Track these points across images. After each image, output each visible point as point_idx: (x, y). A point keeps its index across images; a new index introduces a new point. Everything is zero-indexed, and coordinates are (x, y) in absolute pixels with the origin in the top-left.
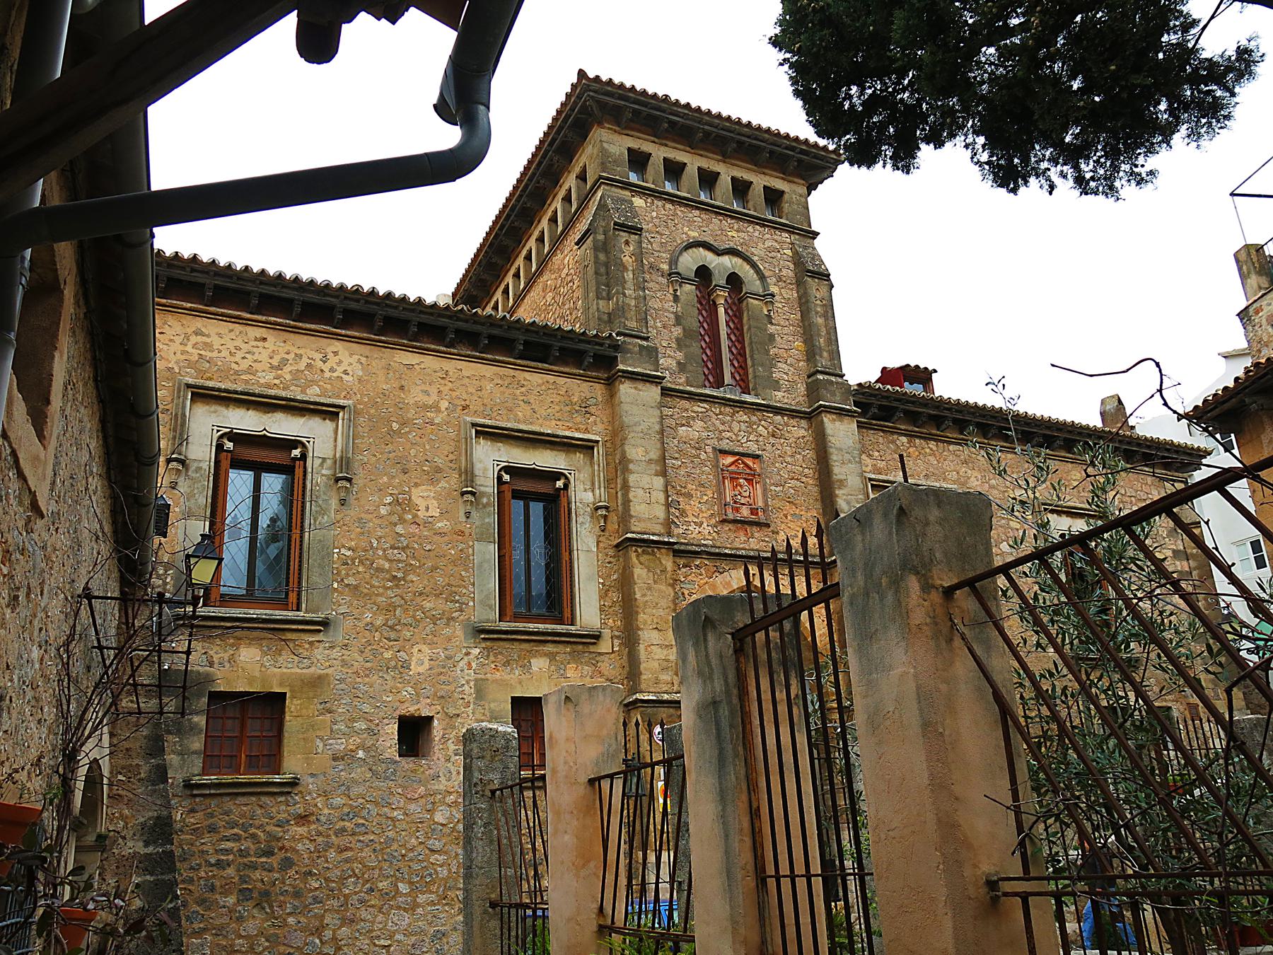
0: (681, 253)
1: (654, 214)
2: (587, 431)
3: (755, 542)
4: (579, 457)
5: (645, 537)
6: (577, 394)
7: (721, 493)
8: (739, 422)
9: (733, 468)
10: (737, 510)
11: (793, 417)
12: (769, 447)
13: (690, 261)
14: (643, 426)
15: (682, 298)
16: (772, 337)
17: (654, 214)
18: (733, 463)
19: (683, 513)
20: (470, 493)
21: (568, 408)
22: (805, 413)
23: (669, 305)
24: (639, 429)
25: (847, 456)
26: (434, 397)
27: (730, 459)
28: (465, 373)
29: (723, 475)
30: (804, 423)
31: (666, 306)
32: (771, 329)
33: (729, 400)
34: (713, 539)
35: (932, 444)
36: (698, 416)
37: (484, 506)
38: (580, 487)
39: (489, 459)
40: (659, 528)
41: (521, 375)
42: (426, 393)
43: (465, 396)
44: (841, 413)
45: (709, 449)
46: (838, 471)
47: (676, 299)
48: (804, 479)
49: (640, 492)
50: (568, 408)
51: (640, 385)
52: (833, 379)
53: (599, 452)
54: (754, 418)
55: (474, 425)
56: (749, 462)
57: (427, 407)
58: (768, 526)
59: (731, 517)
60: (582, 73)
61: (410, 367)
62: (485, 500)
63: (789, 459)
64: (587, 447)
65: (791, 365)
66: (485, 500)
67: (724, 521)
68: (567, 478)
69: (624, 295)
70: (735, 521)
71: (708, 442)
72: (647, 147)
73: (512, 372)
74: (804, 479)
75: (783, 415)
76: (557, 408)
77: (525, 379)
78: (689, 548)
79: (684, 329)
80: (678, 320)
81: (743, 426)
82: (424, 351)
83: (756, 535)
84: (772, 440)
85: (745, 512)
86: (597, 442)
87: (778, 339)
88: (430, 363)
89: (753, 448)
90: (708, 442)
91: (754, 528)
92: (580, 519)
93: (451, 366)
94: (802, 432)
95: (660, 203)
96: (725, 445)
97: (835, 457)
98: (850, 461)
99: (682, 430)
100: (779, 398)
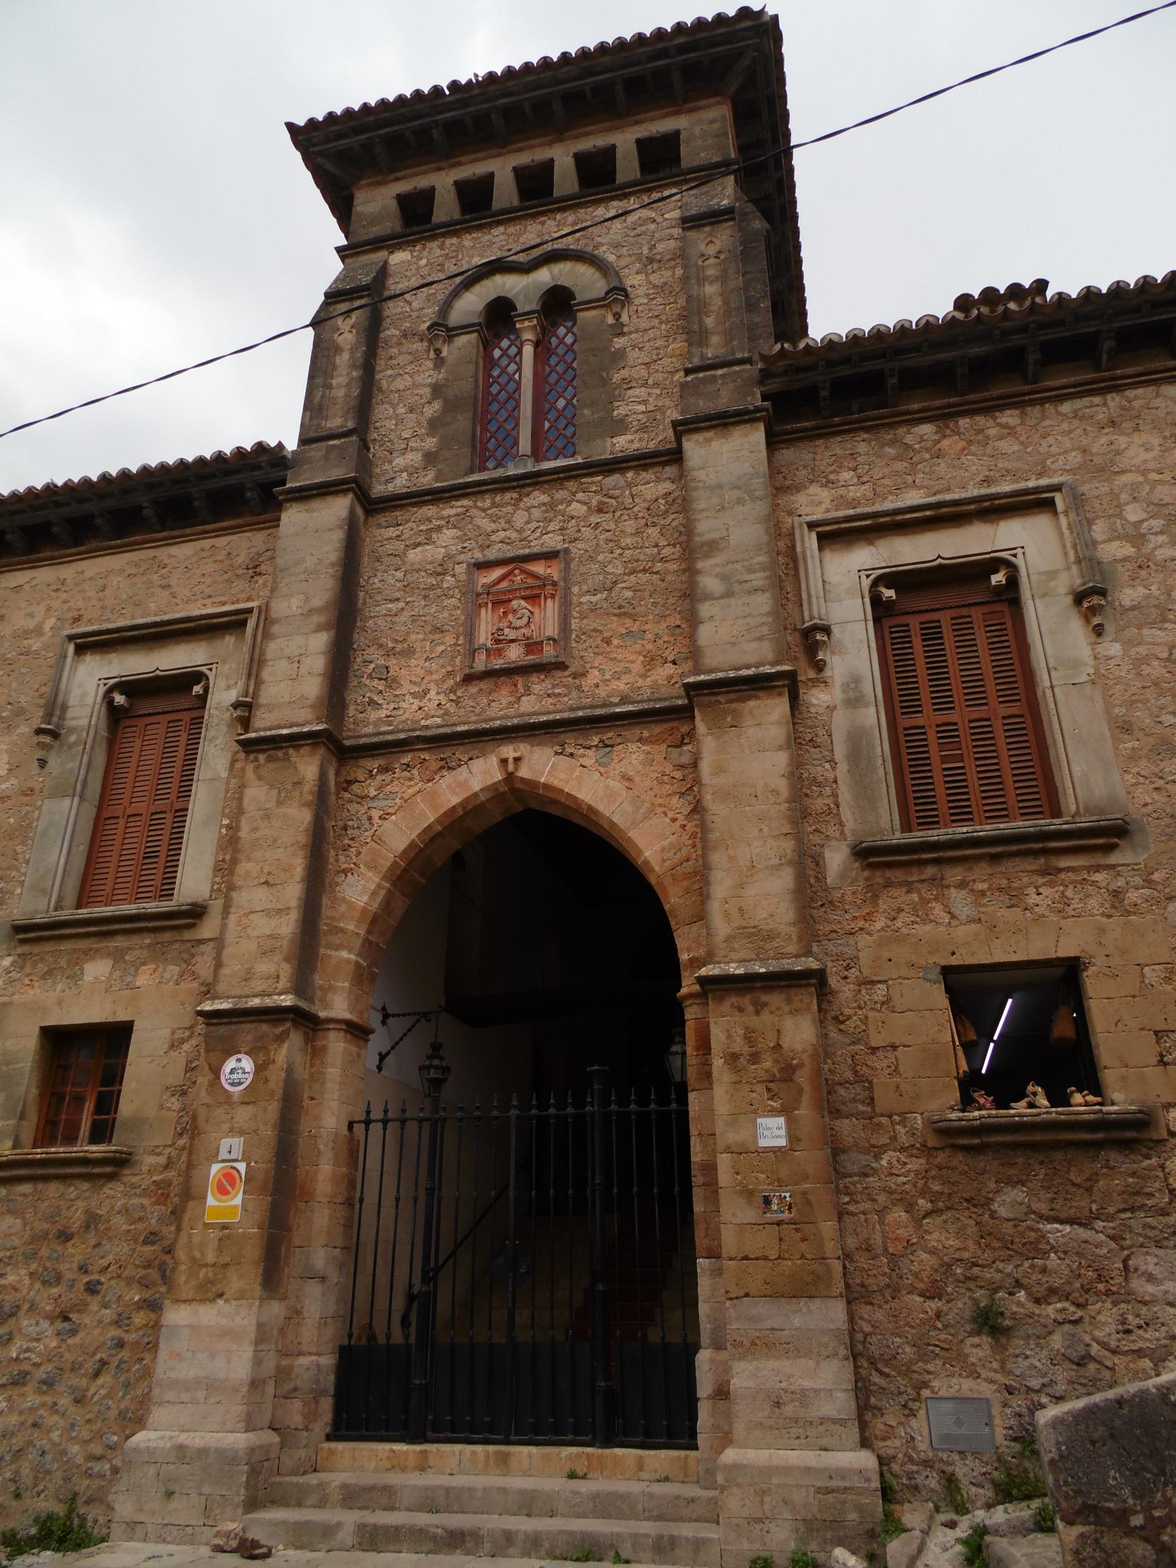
0: (455, 294)
1: (424, 261)
2: (249, 599)
3: (536, 701)
4: (229, 641)
5: (273, 732)
6: (243, 554)
7: (470, 632)
8: (528, 510)
9: (504, 585)
10: (499, 653)
11: (645, 468)
12: (587, 532)
13: (472, 303)
14: (310, 562)
15: (450, 360)
16: (621, 354)
17: (424, 261)
18: (503, 578)
19: (391, 682)
20: (51, 733)
21: (225, 577)
22: (668, 452)
23: (428, 375)
24: (301, 568)
25: (737, 493)
26: (39, 618)
27: (498, 572)
28: (88, 575)
29: (476, 600)
30: (670, 471)
31: (419, 379)
32: (619, 343)
33: (509, 479)
34: (447, 713)
35: (1010, 417)
36: (448, 523)
37: (70, 747)
38: (222, 683)
39: (89, 681)
40: (304, 714)
41: (163, 553)
42: (31, 615)
43: (80, 604)
44: (723, 421)
45: (460, 569)
46: (706, 527)
47: (439, 361)
48: (659, 566)
49: (284, 663)
50: (225, 577)
51: (316, 504)
52: (720, 372)
53: (251, 624)
54: (561, 494)
55: (71, 638)
56: (539, 568)
57: (26, 634)
58: (561, 666)
59: (481, 663)
60: (290, 126)
61: (18, 588)
62: (73, 738)
63: (629, 541)
64: (234, 623)
65: (656, 385)
66: (73, 738)
67: (469, 679)
68: (208, 679)
69: (330, 387)
70: (490, 674)
71: (462, 557)
72: (423, 182)
73: (151, 553)
74: (659, 566)
75: (623, 471)
76: (209, 580)
77: (170, 556)
78: (390, 737)
79: (446, 402)
80: (437, 390)
81: (536, 513)
82: (34, 565)
83: (536, 688)
84: (594, 519)
85: (515, 654)
86: (250, 611)
87: (633, 355)
88: (45, 575)
89: (553, 541)
90: (462, 557)
91: (534, 678)
92: (212, 733)
93: (67, 572)
94: (668, 486)
95: (434, 245)
96: (492, 554)
97: (702, 501)
98: (740, 501)
99: (414, 555)
100: (623, 443)
